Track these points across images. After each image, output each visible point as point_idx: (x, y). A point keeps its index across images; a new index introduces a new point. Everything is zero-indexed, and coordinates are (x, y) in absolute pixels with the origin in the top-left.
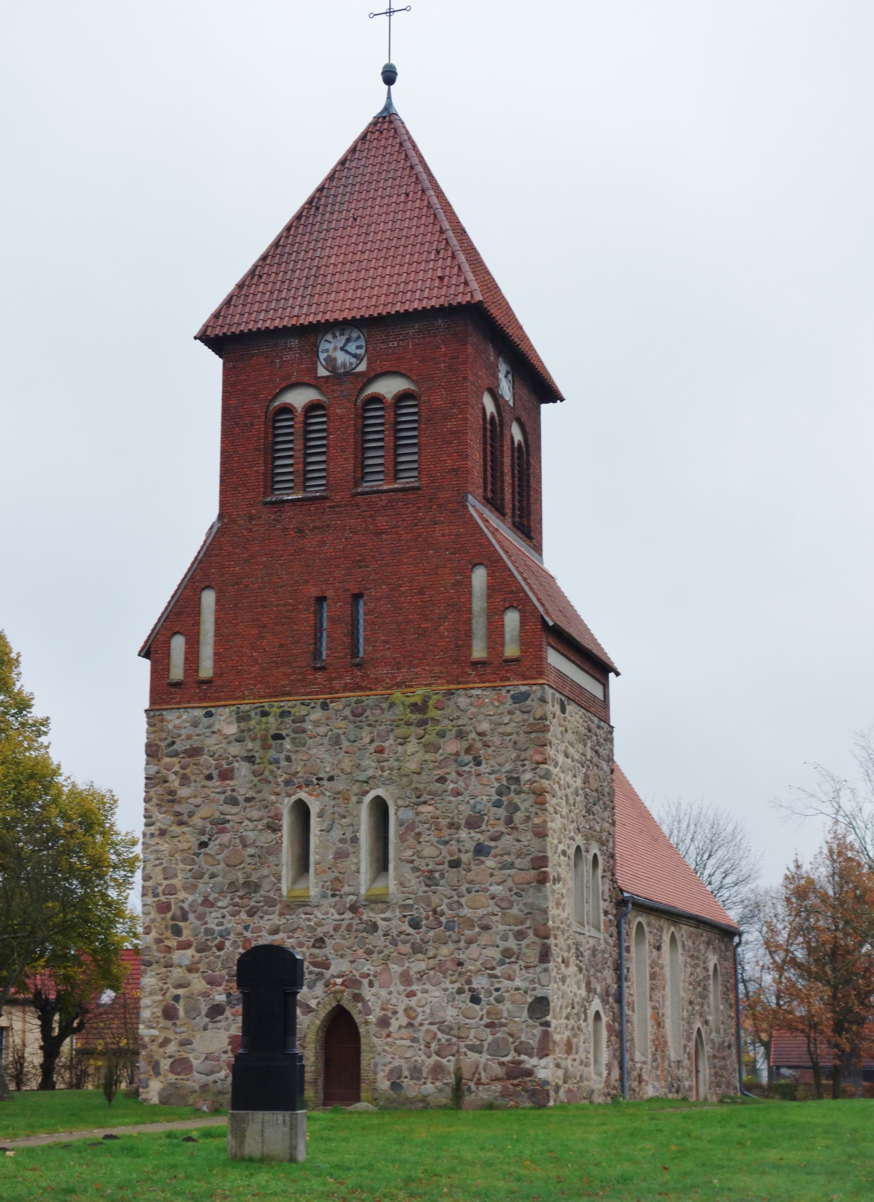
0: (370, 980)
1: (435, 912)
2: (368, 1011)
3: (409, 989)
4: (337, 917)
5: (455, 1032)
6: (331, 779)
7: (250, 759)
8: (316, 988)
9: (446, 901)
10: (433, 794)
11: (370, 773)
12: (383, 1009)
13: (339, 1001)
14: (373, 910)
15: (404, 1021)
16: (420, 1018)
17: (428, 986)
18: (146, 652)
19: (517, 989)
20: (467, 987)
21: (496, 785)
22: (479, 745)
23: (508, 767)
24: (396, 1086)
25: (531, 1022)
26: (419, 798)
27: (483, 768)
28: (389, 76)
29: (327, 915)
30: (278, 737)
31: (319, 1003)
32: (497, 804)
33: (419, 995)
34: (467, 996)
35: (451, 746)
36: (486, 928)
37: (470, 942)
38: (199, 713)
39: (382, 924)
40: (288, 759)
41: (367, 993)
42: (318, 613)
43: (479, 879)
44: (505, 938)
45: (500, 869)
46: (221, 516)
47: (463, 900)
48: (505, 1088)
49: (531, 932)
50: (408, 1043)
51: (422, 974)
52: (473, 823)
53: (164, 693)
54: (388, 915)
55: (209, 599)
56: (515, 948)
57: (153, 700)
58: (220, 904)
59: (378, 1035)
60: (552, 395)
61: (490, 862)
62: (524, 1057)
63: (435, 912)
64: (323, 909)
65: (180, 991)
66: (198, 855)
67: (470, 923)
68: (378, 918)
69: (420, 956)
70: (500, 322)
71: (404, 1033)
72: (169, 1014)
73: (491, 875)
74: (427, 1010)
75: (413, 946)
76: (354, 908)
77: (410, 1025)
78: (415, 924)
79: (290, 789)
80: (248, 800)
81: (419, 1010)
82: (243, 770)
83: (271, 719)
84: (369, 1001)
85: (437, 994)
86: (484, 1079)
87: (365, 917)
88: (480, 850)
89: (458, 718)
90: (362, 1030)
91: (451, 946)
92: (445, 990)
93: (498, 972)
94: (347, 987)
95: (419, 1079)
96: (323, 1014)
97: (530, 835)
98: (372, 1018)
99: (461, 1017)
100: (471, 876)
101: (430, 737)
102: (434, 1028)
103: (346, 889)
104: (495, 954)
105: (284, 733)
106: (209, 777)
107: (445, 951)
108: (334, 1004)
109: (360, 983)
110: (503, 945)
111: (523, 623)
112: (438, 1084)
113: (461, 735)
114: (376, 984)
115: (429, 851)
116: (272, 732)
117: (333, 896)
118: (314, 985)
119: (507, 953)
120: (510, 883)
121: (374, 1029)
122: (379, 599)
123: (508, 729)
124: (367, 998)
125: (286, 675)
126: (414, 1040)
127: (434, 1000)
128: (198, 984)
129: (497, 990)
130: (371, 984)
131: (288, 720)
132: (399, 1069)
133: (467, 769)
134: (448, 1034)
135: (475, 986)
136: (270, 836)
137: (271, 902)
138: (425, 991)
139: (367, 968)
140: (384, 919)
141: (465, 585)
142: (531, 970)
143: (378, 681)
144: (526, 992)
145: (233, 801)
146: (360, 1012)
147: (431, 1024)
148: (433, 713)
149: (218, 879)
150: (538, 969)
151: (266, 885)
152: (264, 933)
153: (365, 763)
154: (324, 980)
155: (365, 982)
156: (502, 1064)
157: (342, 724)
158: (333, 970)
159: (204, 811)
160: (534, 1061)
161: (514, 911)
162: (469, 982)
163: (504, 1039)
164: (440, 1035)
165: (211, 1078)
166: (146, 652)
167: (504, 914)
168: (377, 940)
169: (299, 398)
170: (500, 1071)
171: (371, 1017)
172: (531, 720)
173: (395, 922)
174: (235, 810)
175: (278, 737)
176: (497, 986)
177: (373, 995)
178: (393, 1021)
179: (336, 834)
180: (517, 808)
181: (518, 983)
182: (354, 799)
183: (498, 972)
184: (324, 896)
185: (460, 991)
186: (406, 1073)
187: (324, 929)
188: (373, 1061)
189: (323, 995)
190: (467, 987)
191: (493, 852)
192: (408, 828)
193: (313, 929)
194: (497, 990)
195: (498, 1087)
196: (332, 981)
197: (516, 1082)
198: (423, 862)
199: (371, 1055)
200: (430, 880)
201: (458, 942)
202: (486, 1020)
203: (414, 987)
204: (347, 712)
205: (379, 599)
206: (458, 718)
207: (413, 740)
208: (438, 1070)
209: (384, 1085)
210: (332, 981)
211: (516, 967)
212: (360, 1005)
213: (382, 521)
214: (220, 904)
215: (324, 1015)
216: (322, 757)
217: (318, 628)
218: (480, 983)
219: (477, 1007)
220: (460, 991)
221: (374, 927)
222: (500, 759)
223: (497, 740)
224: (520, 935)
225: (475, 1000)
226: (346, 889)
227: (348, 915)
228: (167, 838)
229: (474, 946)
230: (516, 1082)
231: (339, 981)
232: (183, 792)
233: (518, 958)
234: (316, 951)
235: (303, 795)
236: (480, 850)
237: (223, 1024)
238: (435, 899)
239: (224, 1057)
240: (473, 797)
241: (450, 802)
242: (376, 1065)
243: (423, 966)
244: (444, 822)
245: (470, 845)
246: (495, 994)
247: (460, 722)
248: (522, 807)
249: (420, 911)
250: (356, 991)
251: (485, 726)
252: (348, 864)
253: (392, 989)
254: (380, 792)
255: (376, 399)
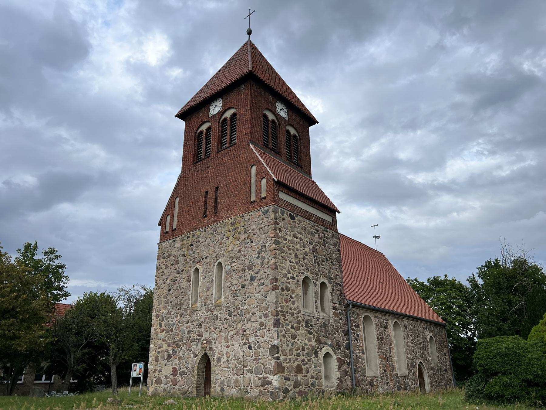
1: (237, 308)
3: (228, 344)
4: (206, 314)
5: (242, 363)
6: (206, 258)
7: (184, 255)
9: (241, 303)
10: (237, 258)
11: (217, 253)
12: (219, 354)
14: (217, 310)
15: (225, 359)
16: (231, 357)
17: (234, 342)
18: (160, 224)
19: (265, 341)
20: (247, 342)
21: (258, 250)
22: (252, 234)
23: (261, 242)
24: (222, 390)
25: (270, 357)
26: (232, 260)
27: (253, 244)
28: (249, 33)
29: (203, 314)
30: (191, 245)
32: (258, 258)
33: (231, 346)
34: (247, 346)
35: (243, 236)
36: (253, 314)
37: (248, 321)
38: (171, 241)
39: (219, 315)
40: (194, 253)
41: (214, 346)
42: (206, 198)
43: (251, 292)
44: (260, 318)
45: (259, 286)
46: (181, 173)
47: (246, 302)
48: (261, 391)
49: (270, 314)
50: (226, 369)
51: (232, 336)
52: (250, 268)
53: (164, 236)
54: (221, 311)
55: (177, 200)
56: (264, 322)
57: (161, 240)
58: (172, 313)
60: (313, 121)
61: (255, 284)
62: (268, 375)
63: (237, 308)
64: (202, 311)
65: (160, 350)
66: (168, 294)
67: (248, 312)
68: (218, 313)
69: (231, 329)
70: (259, 76)
71: (226, 365)
72: (157, 359)
73: (256, 289)
74: (233, 353)
75: (229, 325)
76: (211, 310)
77: (228, 360)
78: (230, 315)
79: (194, 264)
80: (182, 271)
81: (231, 353)
82: (181, 259)
83: (190, 239)
85: (237, 346)
86: (253, 387)
87: (214, 314)
88: (252, 279)
89: (245, 225)
91: (242, 323)
92: (240, 344)
93: (258, 334)
95: (230, 386)
97: (269, 269)
98: (215, 358)
99: (245, 356)
100: (249, 291)
101: (237, 235)
102: (235, 362)
103: (209, 302)
104: (256, 325)
105: (193, 243)
106: (173, 265)
107: (239, 325)
110: (260, 321)
111: (267, 183)
112: (237, 388)
113: (246, 232)
114: (217, 342)
115: (235, 282)
116: (190, 244)
117: (205, 305)
119: (262, 325)
120: (262, 292)
121: (215, 363)
122: (223, 187)
123: (261, 226)
125: (196, 222)
126: (229, 368)
127: (236, 348)
128: (165, 346)
129: (258, 342)
131: (194, 238)
132: (223, 382)
133: (248, 245)
134: (240, 364)
135: (250, 341)
136: (188, 284)
137: (186, 310)
138: (233, 345)
139: (215, 335)
140: (221, 314)
141: (249, 175)
142: (270, 332)
143: (221, 217)
144: (268, 343)
145: (178, 272)
147: (234, 360)
148: (238, 225)
149: (173, 303)
150: (273, 331)
151: (185, 304)
152: (184, 324)
153: (216, 250)
155: (213, 341)
156: (259, 379)
157: (209, 236)
158: (203, 338)
159: (170, 278)
160: (272, 377)
161: (264, 305)
162: (248, 339)
163: (260, 366)
164: (237, 365)
165: (166, 386)
166: (160, 224)
167: (260, 306)
168: (218, 323)
169: (204, 128)
170: (259, 383)
172: (269, 220)
173: (224, 314)
174: (178, 275)
175: (191, 245)
176: (258, 340)
178: (222, 359)
179: (207, 280)
180: (264, 258)
181: (265, 339)
182: (212, 264)
183: (258, 334)
184: (202, 306)
185: (245, 344)
186: (226, 384)
187: (201, 320)
190: (247, 342)
191: (257, 278)
192: (229, 273)
193: (198, 320)
194: (258, 342)
195: (257, 390)
197: (265, 388)
198: (233, 287)
200: (235, 295)
201: (244, 321)
202: (254, 357)
203: (229, 343)
204: (212, 231)
205: (223, 187)
206: (245, 225)
207: (231, 237)
208: (236, 381)
209: (218, 389)
211: (265, 331)
213: (225, 159)
214: (172, 313)
216: (204, 251)
217: (206, 204)
218: (252, 339)
219: (251, 351)
220: (245, 344)
221: (217, 317)
222: (259, 239)
223: (258, 231)
224: (266, 315)
225: (250, 348)
226: (209, 302)
227: (209, 313)
228: (160, 289)
229: (249, 322)
230: (265, 388)
231: (205, 342)
232: (165, 271)
233: (265, 327)
234: (199, 329)
235: (198, 266)
236: (252, 279)
237: (171, 362)
238: (237, 303)
239: (171, 376)
240: (250, 256)
241: (242, 260)
243: (232, 333)
244: (240, 269)
245: (248, 277)
246: (257, 344)
247: (246, 227)
248: (266, 257)
249: (233, 309)
251: (254, 227)
252: (209, 292)
253: (222, 344)
254: (220, 260)
255: (225, 119)
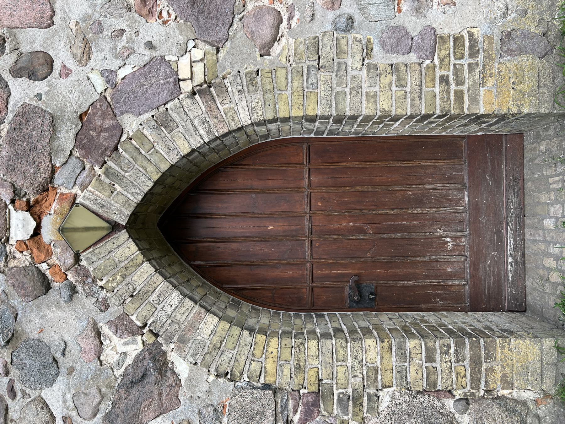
0: (16, 72)
2: (159, 73)
8: (52, 338)
13: (115, 227)
31: (122, 325)
41: (73, 89)
59: (266, 33)
84: (109, 76)
90: (242, 111)
94: (46, 188)
96: (171, 304)
108: (126, 248)
109: (26, 114)
114: (33, 40)
118: (38, 348)
124: (100, 84)
130: (38, 67)
146: (164, 123)
154: (16, 301)
171: (184, 73)
177: (85, 56)
188: (380, 57)
189: (86, 304)
196: (23, 259)
199: (353, 61)
210: (23, 259)
212: (131, 124)
215: (175, 297)
242: (398, 40)
250: (66, 138)
